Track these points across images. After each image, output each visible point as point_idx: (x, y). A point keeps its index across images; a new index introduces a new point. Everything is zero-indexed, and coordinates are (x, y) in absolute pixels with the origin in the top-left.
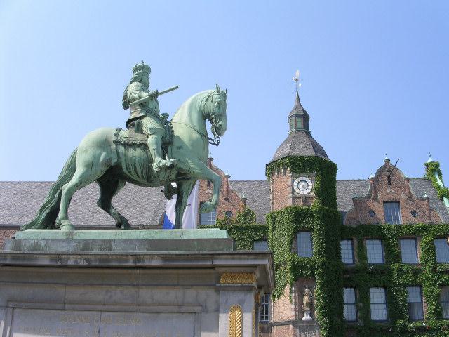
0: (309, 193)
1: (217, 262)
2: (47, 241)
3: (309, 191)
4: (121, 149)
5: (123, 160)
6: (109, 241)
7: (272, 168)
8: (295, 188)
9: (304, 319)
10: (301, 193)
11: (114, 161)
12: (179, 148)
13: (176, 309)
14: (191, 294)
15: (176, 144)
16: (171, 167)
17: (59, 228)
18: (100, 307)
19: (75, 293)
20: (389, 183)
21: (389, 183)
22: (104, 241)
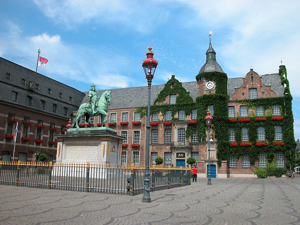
0: (212, 88)
1: (100, 136)
2: (72, 131)
3: (212, 87)
5: (87, 111)
6: (84, 131)
7: (199, 78)
8: (207, 86)
9: (210, 141)
10: (209, 88)
11: (86, 112)
14: (97, 142)
17: (76, 128)
18: (82, 145)
19: (77, 142)
20: (252, 80)
21: (252, 80)
22: (83, 131)
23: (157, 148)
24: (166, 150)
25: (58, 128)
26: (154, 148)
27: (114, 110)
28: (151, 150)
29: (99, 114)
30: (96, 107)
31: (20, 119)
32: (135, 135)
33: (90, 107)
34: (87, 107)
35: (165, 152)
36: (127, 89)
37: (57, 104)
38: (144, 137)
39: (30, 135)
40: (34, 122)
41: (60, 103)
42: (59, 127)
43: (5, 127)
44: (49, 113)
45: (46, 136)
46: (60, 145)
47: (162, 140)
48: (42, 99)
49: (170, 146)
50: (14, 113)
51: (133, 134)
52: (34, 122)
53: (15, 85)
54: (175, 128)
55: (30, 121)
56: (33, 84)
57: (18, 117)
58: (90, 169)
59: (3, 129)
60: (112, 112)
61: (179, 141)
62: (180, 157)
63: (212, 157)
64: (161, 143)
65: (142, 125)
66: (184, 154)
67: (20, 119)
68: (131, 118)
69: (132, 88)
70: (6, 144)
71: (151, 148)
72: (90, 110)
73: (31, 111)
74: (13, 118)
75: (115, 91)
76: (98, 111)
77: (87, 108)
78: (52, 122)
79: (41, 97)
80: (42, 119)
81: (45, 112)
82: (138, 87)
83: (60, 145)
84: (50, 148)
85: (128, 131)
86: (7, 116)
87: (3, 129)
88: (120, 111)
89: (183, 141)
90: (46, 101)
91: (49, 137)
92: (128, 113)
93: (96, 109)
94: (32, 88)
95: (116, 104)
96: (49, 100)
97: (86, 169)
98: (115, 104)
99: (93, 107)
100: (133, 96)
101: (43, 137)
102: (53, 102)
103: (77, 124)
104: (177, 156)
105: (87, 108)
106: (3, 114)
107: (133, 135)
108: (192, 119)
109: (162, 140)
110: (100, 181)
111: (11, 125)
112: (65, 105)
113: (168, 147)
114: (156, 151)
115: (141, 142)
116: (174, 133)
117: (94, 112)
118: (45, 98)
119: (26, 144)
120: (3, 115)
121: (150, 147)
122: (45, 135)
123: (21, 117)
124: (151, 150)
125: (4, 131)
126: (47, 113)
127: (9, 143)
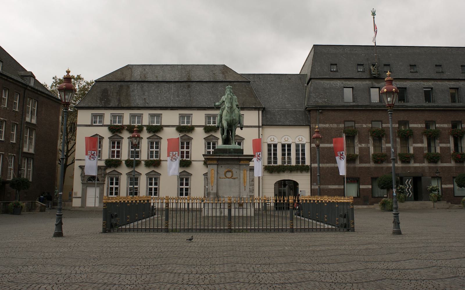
25: (444, 129)
31: (364, 126)
37: (433, 86)
39: (389, 149)
41: (440, 83)
42: (446, 126)
44: (416, 107)
45: (420, 145)
48: (398, 86)
50: (353, 119)
53: (347, 77)
56: (375, 68)
57: (360, 123)
67: (364, 126)
73: (379, 110)
78: (428, 119)
80: (406, 119)
81: (407, 107)
84: (432, 165)
90: (407, 87)
91: (426, 146)
94: (375, 74)
96: (416, 83)
101: (415, 148)
102: (424, 85)
106: (336, 123)
112: (452, 84)
118: (405, 83)
122: (418, 143)
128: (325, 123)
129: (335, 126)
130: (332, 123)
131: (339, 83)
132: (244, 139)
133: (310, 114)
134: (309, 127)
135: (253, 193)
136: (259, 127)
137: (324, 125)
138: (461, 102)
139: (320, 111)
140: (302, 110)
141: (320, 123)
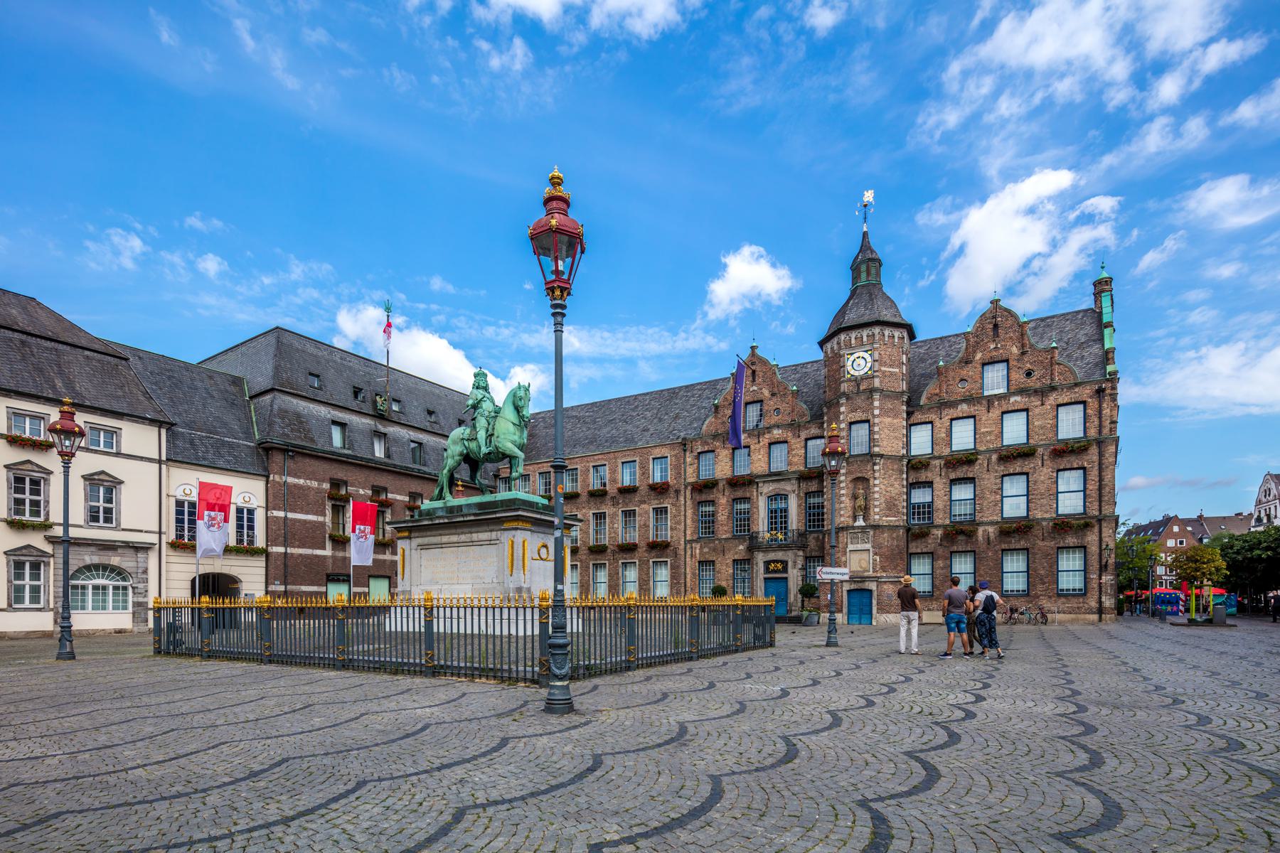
4: (466, 443)
9: (857, 524)
11: (465, 452)
12: (498, 437)
13: (488, 543)
15: (496, 434)
16: (489, 453)
23: (714, 550)
24: (736, 553)
26: (706, 550)
27: (600, 457)
28: (698, 556)
29: (500, 456)
30: (490, 436)
31: (361, 492)
32: (657, 519)
33: (473, 439)
34: (466, 436)
35: (734, 560)
36: (635, 399)
38: (678, 523)
40: (399, 497)
43: (324, 515)
46: (404, 550)
47: (726, 528)
48: (412, 438)
49: (747, 543)
50: (345, 478)
51: (651, 515)
52: (399, 497)
54: (761, 493)
55: (390, 496)
57: (356, 487)
58: (435, 610)
59: (321, 519)
60: (596, 461)
61: (772, 530)
62: (775, 571)
63: (861, 567)
64: (724, 537)
65: (672, 491)
66: (785, 563)
67: (361, 492)
68: (643, 474)
69: (648, 394)
70: (333, 557)
71: (698, 551)
72: (473, 445)
74: (343, 492)
75: (603, 406)
76: (497, 448)
77: (468, 440)
79: (411, 433)
80: (419, 491)
81: (425, 473)
82: (662, 391)
83: (404, 550)
85: (637, 508)
86: (326, 486)
87: (321, 519)
88: (616, 458)
89: (781, 527)
92: (635, 461)
93: (490, 442)
95: (606, 441)
97: (536, 611)
98: (603, 440)
99: (482, 435)
100: (649, 414)
103: (446, 490)
104: (767, 570)
105: (468, 440)
107: (651, 520)
108: (806, 467)
109: (726, 528)
110: (521, 642)
111: (341, 508)
113: (741, 547)
114: (711, 559)
115: (672, 537)
116: (757, 508)
117: (484, 450)
119: (385, 554)
120: (316, 483)
121: (695, 548)
123: (363, 488)
124: (698, 556)
125: (323, 524)
126: (430, 474)
127: (340, 554)
128: (299, 477)
129: (315, 484)
130: (311, 479)
131: (323, 411)
132: (121, 482)
133: (267, 455)
134: (264, 479)
135: (145, 596)
136: (160, 462)
137: (296, 480)
138: (485, 479)
139: (290, 454)
140: (252, 444)
141: (289, 475)
